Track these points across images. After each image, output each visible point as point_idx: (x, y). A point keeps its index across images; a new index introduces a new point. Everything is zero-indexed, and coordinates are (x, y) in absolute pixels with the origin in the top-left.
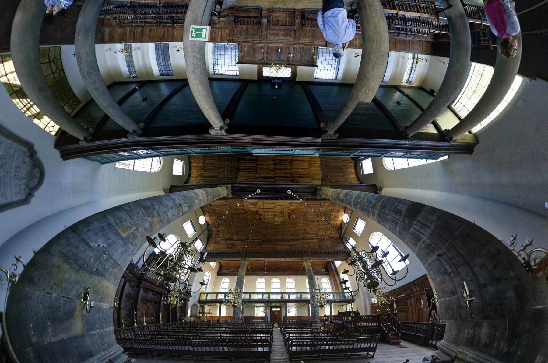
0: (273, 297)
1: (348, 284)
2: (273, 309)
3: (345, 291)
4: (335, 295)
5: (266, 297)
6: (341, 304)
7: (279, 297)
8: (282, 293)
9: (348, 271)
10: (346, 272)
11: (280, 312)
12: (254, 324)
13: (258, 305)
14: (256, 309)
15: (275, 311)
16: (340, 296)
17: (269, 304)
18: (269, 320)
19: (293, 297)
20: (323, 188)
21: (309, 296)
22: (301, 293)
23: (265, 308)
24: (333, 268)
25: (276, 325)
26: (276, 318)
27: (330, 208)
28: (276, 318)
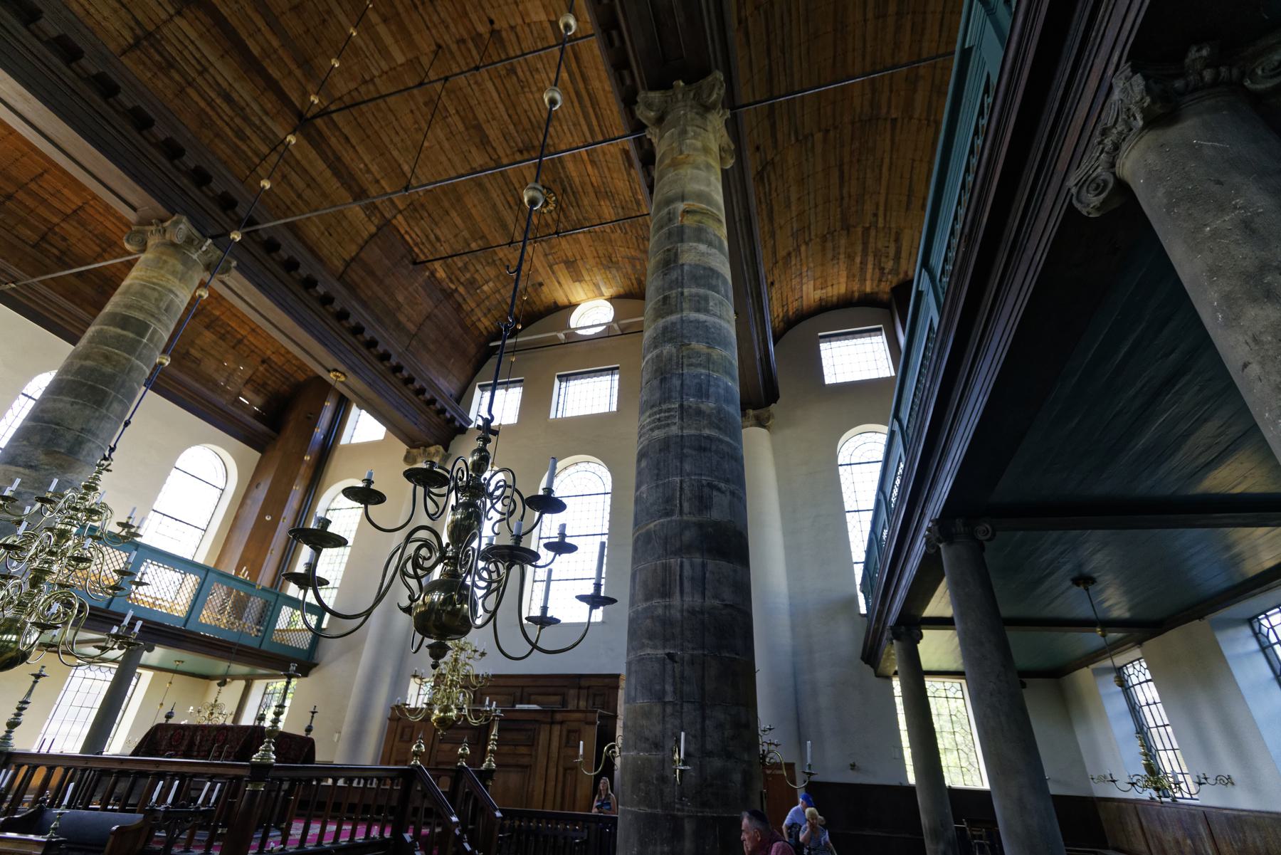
1: (331, 564)
3: (293, 590)
4: (218, 594)
6: (221, 666)
9: (379, 498)
10: (366, 495)
16: (239, 608)
20: (717, 120)
24: (319, 433)
27: (608, 212)
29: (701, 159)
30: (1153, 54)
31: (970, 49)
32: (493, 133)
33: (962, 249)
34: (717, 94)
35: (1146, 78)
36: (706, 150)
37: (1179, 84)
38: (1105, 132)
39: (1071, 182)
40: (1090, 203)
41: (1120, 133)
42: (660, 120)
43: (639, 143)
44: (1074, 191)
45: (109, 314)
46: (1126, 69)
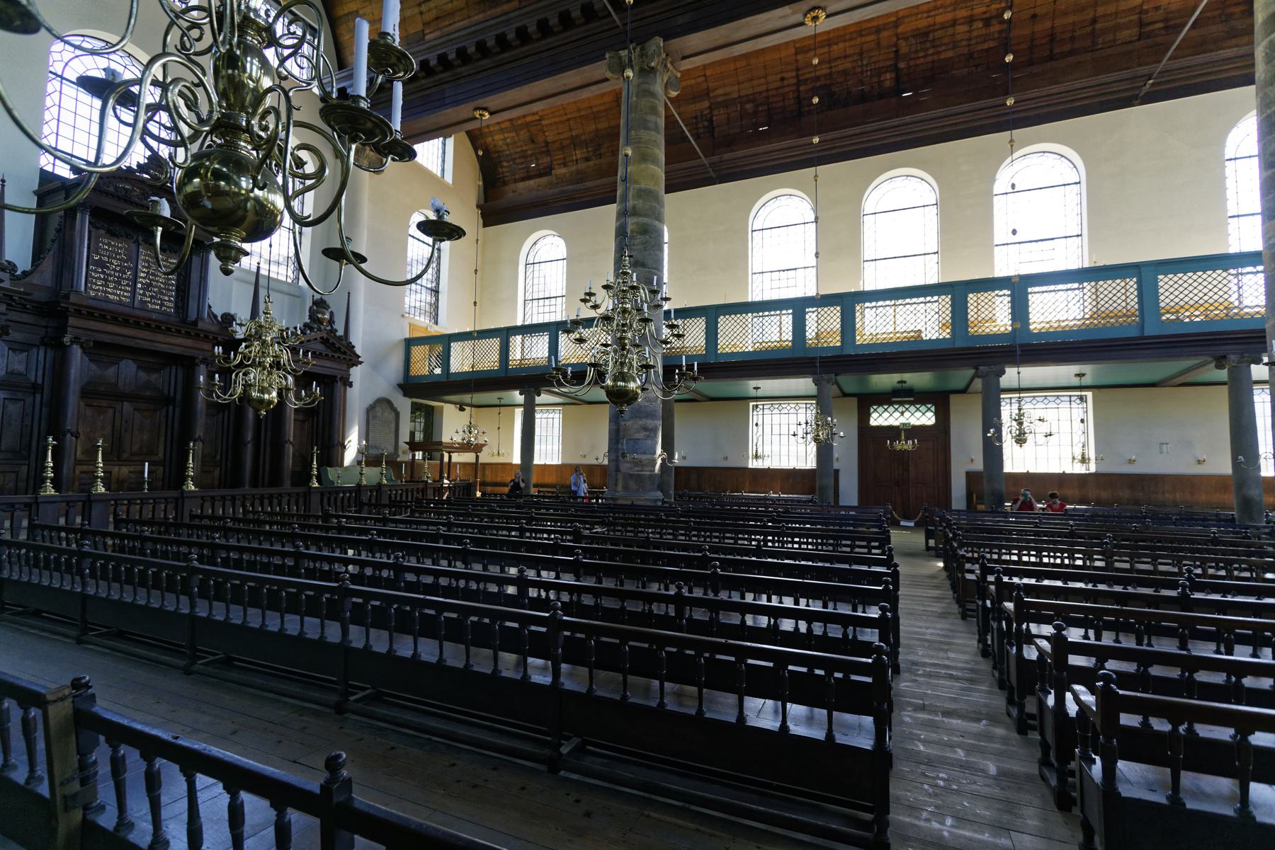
0: (876, 325)
2: (882, 418)
5: (823, 327)
7: (927, 322)
8: (958, 293)
11: (937, 437)
12: (746, 516)
13: (769, 386)
14: (755, 417)
15: (893, 432)
17: (849, 382)
18: (849, 493)
19: (1055, 310)
21: (1249, 294)
22: (1145, 274)
23: (823, 409)
25: (905, 537)
26: (900, 480)
28: (900, 480)
45: (1265, 23)
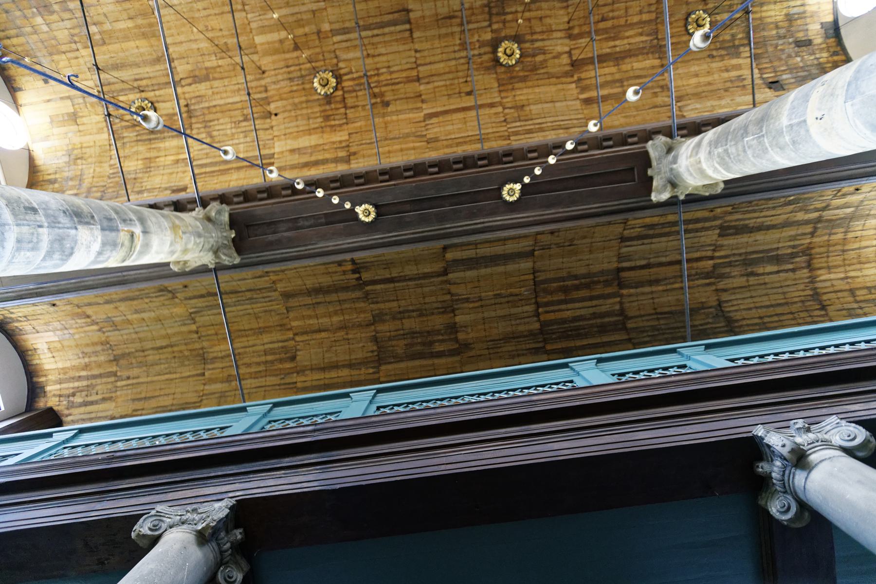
20: (208, 259)
29: (179, 247)
30: (242, 512)
31: (246, 411)
32: (202, 88)
33: (100, 457)
34: (226, 260)
35: (227, 516)
36: (185, 251)
37: (223, 534)
38: (195, 510)
39: (159, 508)
40: (143, 527)
41: (194, 519)
42: (209, 219)
43: (193, 201)
44: (153, 512)
46: (233, 501)
